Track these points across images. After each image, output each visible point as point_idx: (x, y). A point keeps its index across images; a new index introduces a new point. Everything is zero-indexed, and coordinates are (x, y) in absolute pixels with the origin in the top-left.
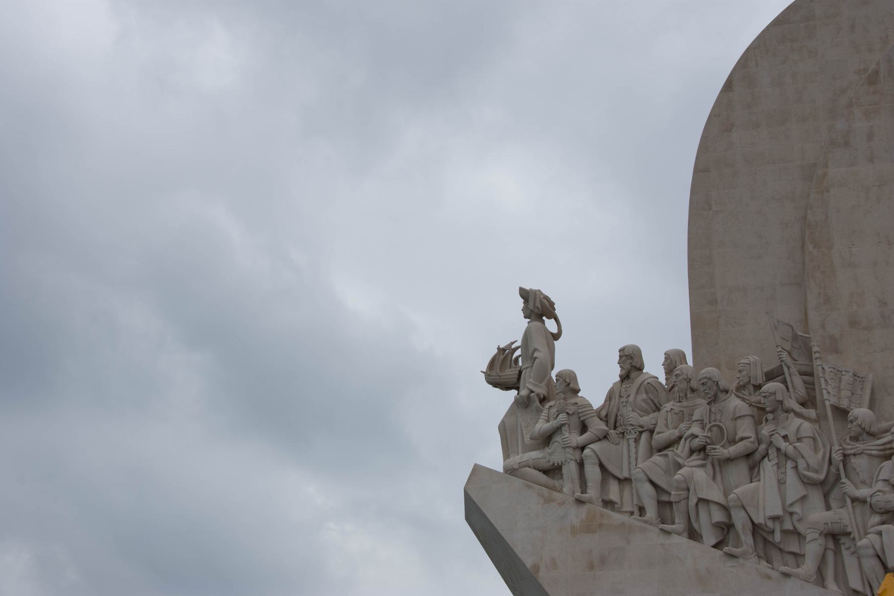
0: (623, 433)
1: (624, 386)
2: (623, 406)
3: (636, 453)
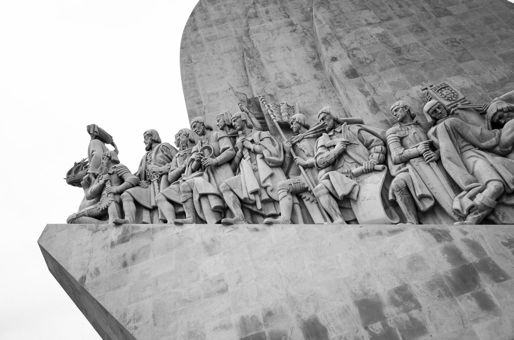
0: (150, 181)
3: (159, 189)
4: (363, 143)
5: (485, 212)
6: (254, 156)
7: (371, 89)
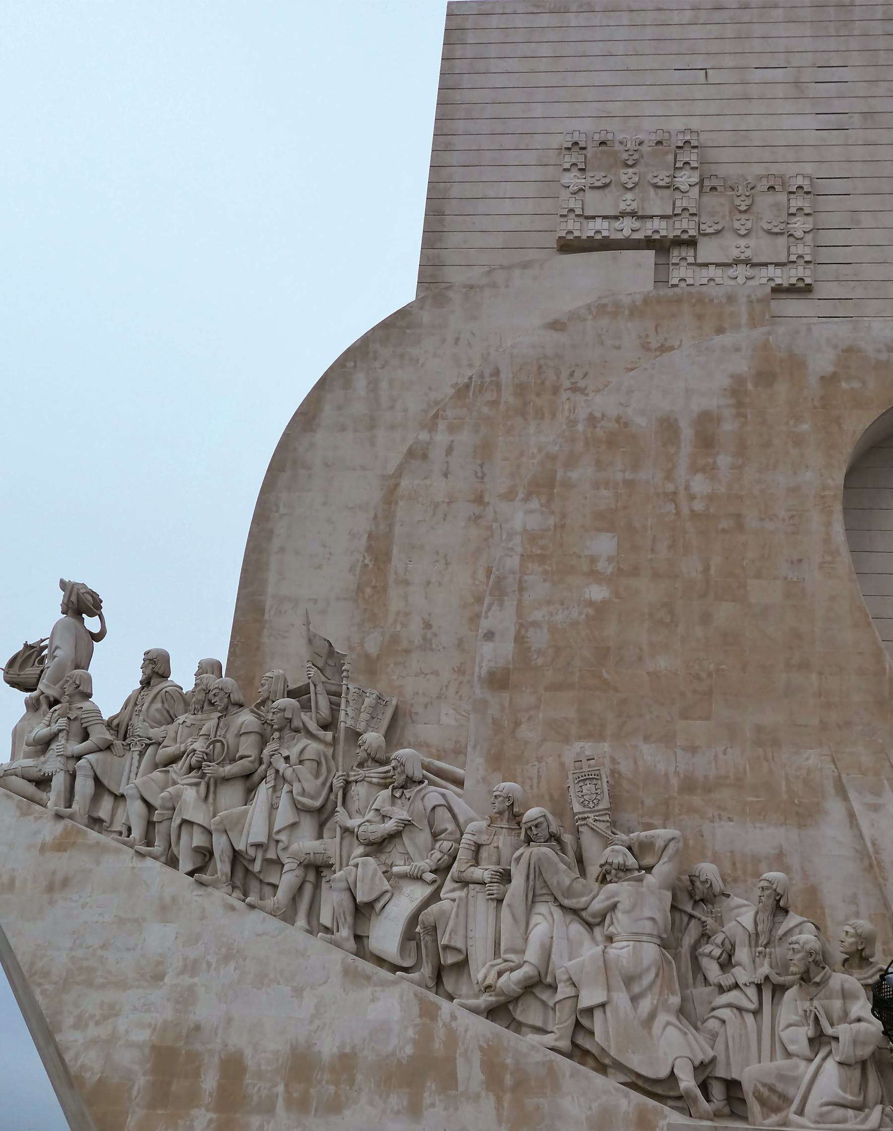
1: (142, 694)
2: (136, 715)
3: (138, 767)
4: (431, 828)
5: (502, 999)
6: (282, 782)
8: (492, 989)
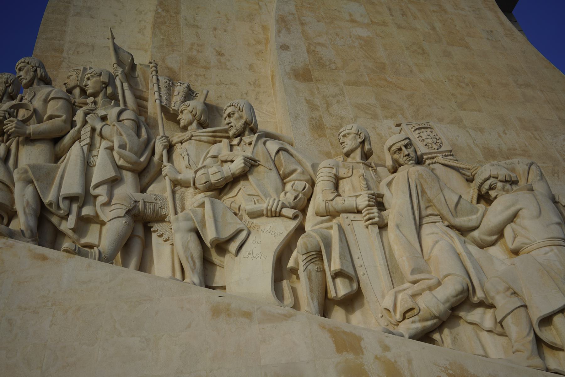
7: (324, 103)
8: (416, 311)
